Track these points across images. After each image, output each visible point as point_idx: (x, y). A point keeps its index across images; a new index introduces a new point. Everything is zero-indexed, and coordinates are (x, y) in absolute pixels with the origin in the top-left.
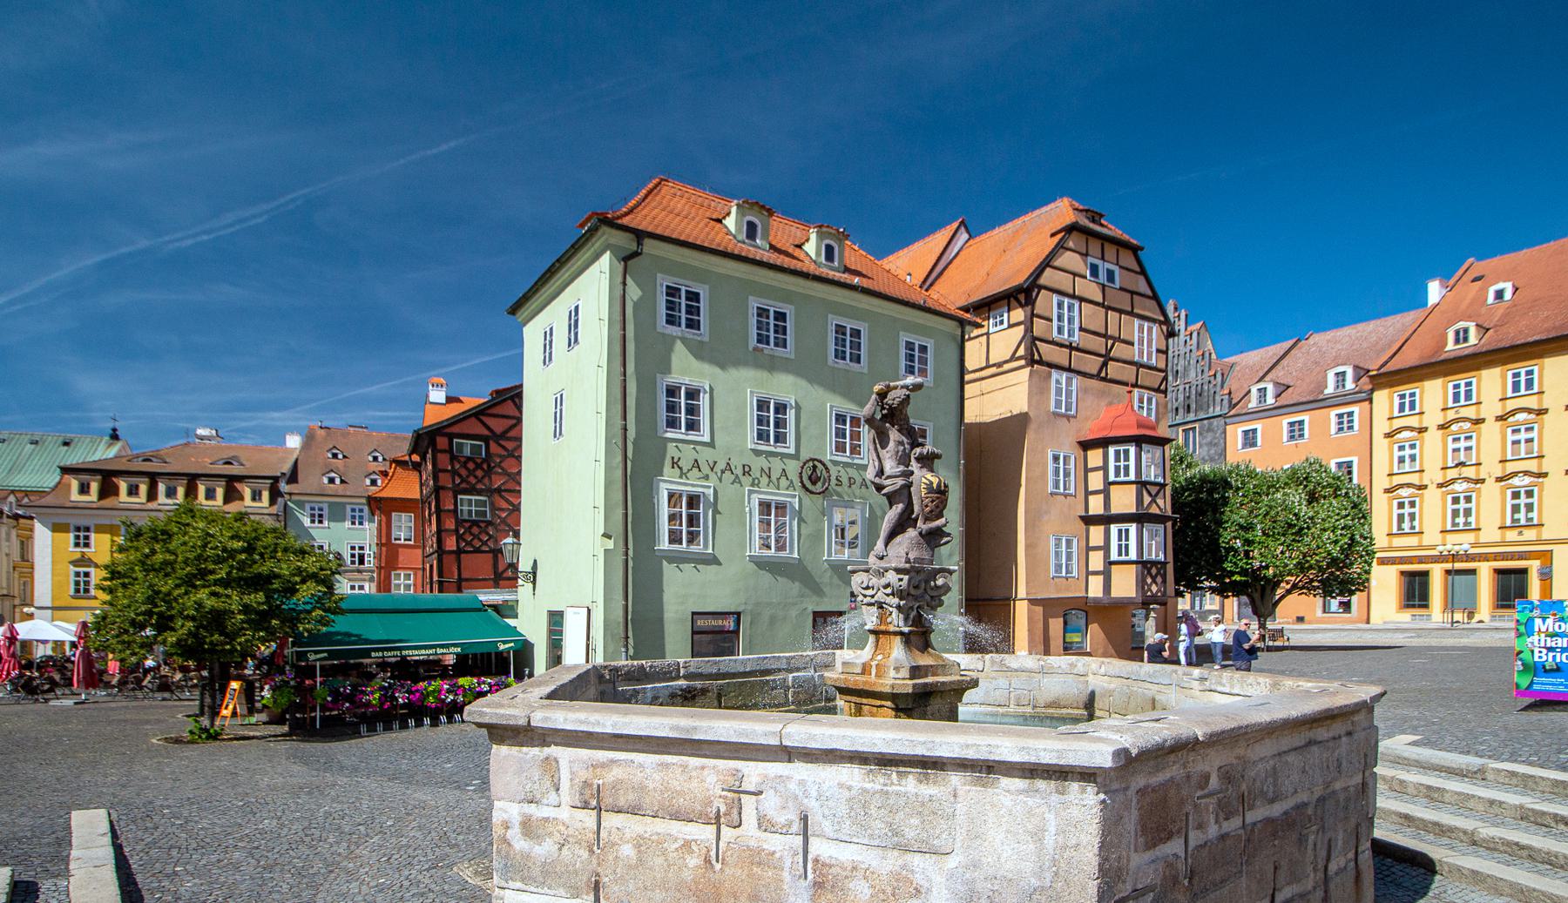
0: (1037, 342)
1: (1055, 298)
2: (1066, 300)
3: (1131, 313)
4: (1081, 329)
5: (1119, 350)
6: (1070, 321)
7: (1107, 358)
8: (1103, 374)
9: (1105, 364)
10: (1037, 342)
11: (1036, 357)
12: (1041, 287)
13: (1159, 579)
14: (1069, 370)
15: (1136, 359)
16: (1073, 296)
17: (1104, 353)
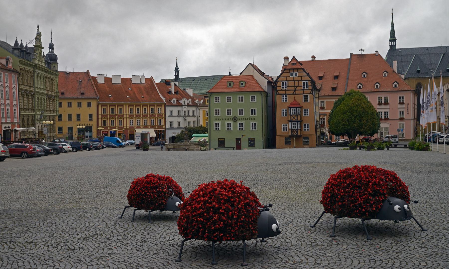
0: (278, 91)
1: (282, 82)
2: (284, 82)
3: (302, 80)
4: (288, 86)
5: (298, 88)
6: (286, 85)
7: (295, 90)
8: (294, 93)
9: (295, 92)
10: (278, 91)
11: (278, 93)
12: (278, 81)
13: (296, 132)
14: (286, 94)
15: (303, 89)
16: (286, 81)
17: (294, 89)
